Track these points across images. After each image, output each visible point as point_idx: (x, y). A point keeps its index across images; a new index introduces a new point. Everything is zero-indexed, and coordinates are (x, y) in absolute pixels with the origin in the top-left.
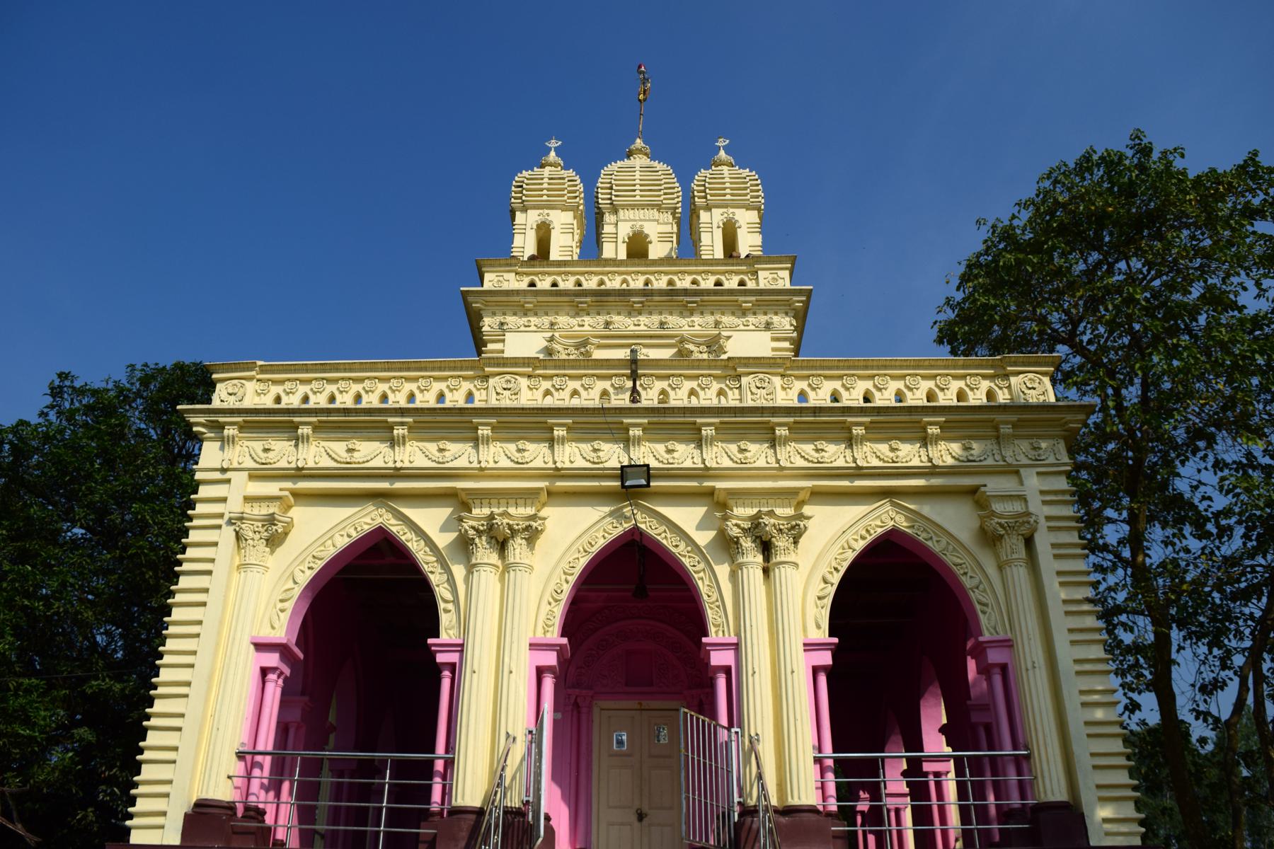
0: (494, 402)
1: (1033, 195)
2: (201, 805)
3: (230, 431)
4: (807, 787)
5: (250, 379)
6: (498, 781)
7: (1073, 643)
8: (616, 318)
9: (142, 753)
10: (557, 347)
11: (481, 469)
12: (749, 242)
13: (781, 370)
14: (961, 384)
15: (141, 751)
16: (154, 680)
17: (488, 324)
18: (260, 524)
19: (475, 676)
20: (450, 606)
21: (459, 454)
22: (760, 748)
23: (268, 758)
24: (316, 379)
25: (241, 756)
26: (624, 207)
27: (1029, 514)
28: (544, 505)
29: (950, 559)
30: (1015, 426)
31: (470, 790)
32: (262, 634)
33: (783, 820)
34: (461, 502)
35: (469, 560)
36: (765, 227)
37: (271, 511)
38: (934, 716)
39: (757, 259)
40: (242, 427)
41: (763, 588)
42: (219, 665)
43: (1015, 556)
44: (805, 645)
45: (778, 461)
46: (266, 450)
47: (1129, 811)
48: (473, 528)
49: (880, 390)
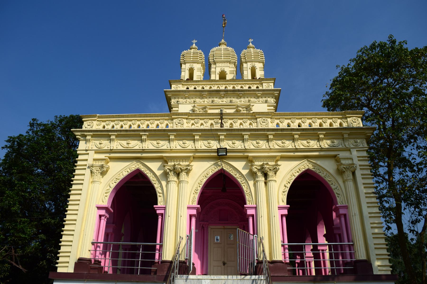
0: (175, 128)
1: (355, 57)
2: (80, 260)
3: (88, 138)
4: (279, 254)
5: (95, 120)
6: (177, 252)
7: (368, 207)
8: (215, 99)
9: (61, 243)
10: (196, 109)
11: (171, 150)
12: (260, 74)
13: (270, 116)
14: (331, 121)
15: (61, 242)
16: (64, 219)
17: (173, 101)
18: (98, 168)
19: (169, 217)
20: (161, 195)
21: (164, 145)
22: (263, 241)
23: (102, 244)
24: (116, 120)
26: (218, 62)
27: (353, 164)
28: (192, 161)
29: (327, 179)
30: (349, 135)
31: (168, 255)
32: (99, 204)
33: (271, 265)
34: (165, 160)
35: (167, 180)
36: (265, 68)
37: (102, 164)
38: (322, 231)
40: (92, 136)
41: (265, 189)
42: (85, 214)
43: (349, 178)
44: (278, 207)
45: (269, 147)
46: (100, 144)
47: (387, 263)
48: (168, 169)
49: (303, 123)
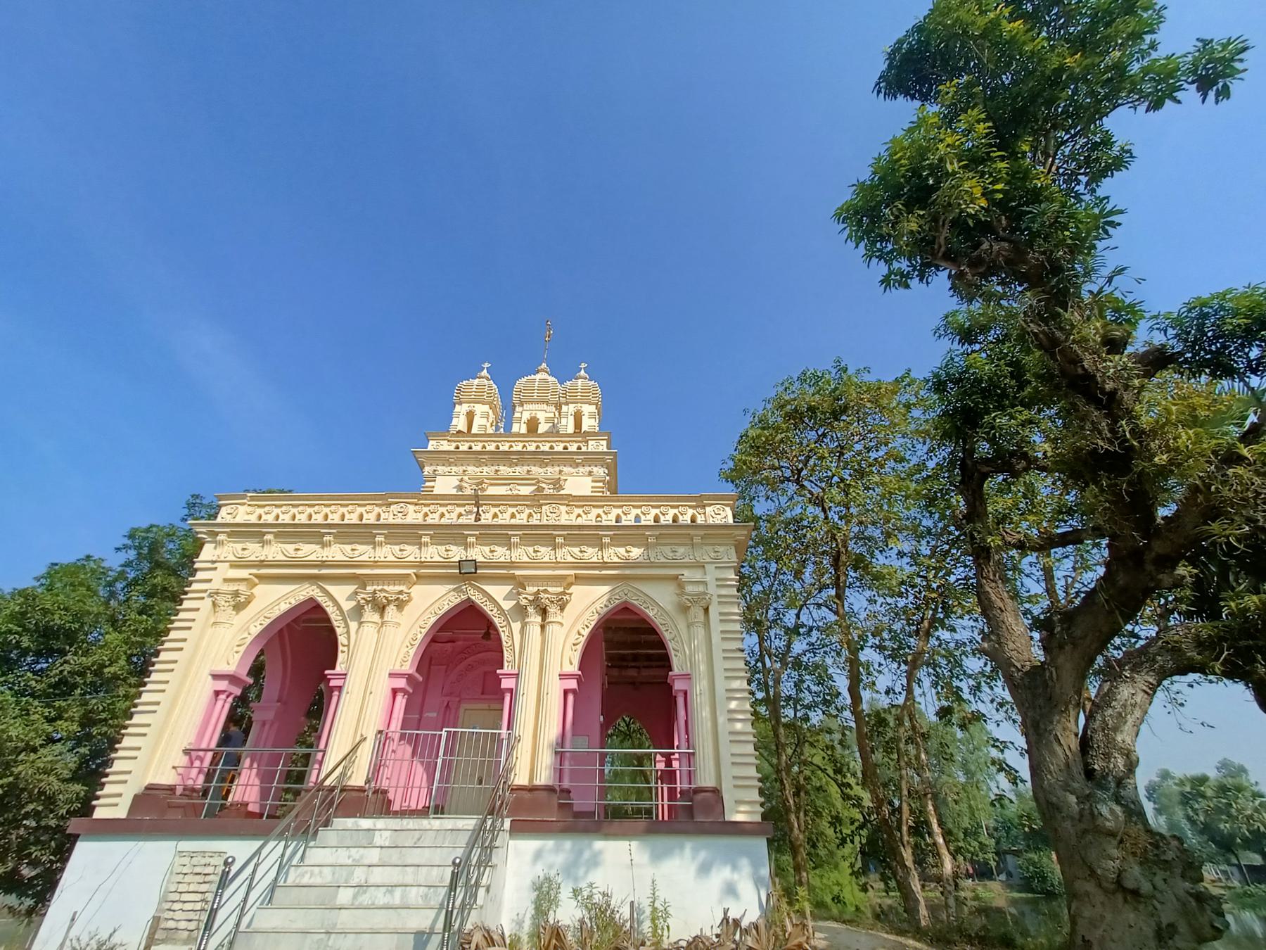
0: (391, 521)
2: (150, 788)
3: (221, 537)
8: (501, 468)
12: (588, 423)
21: (364, 552)
25: (187, 752)
39: (594, 434)
40: (230, 535)
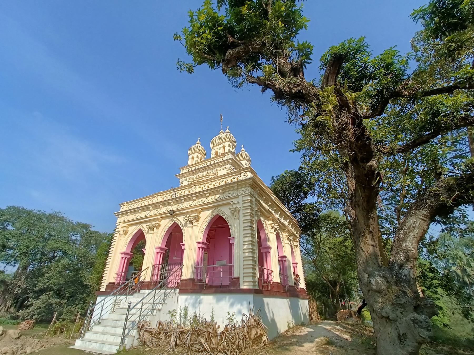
2: (110, 283)
25: (117, 274)
40: (122, 215)
